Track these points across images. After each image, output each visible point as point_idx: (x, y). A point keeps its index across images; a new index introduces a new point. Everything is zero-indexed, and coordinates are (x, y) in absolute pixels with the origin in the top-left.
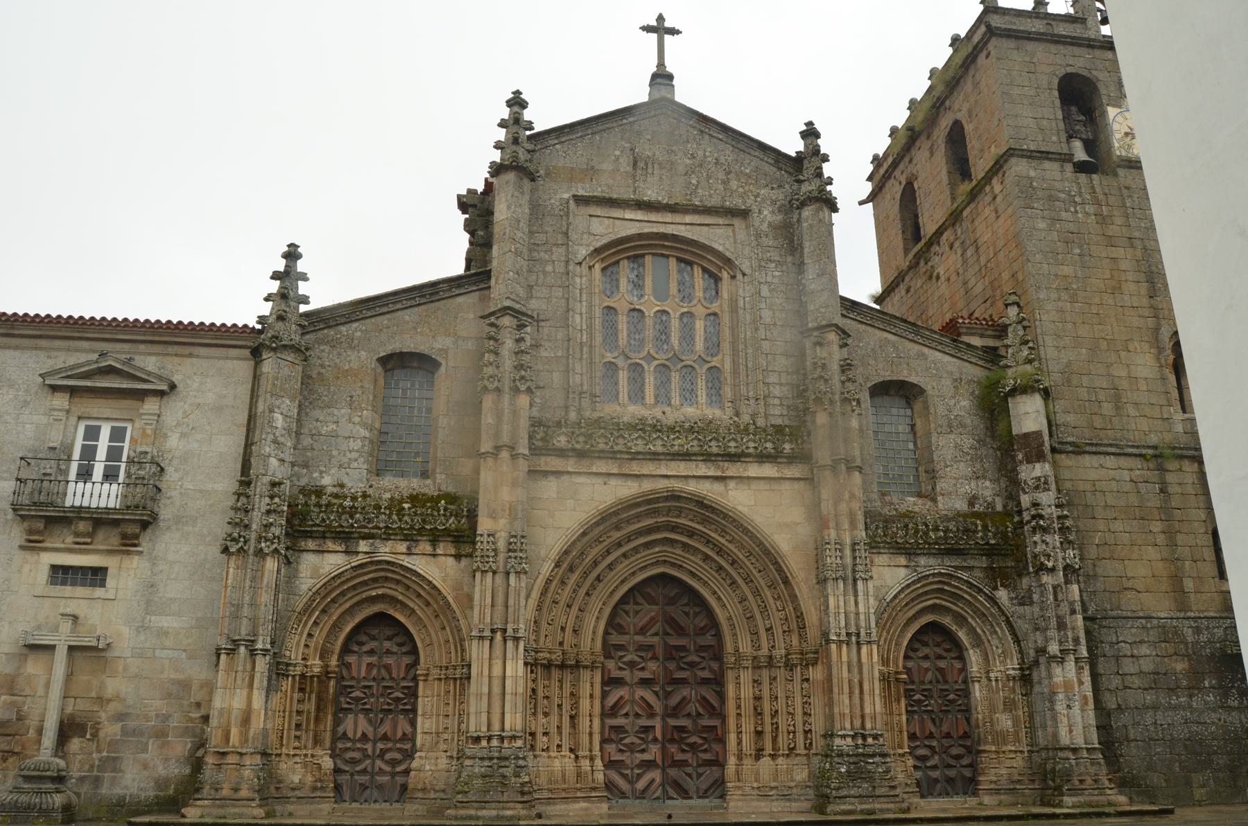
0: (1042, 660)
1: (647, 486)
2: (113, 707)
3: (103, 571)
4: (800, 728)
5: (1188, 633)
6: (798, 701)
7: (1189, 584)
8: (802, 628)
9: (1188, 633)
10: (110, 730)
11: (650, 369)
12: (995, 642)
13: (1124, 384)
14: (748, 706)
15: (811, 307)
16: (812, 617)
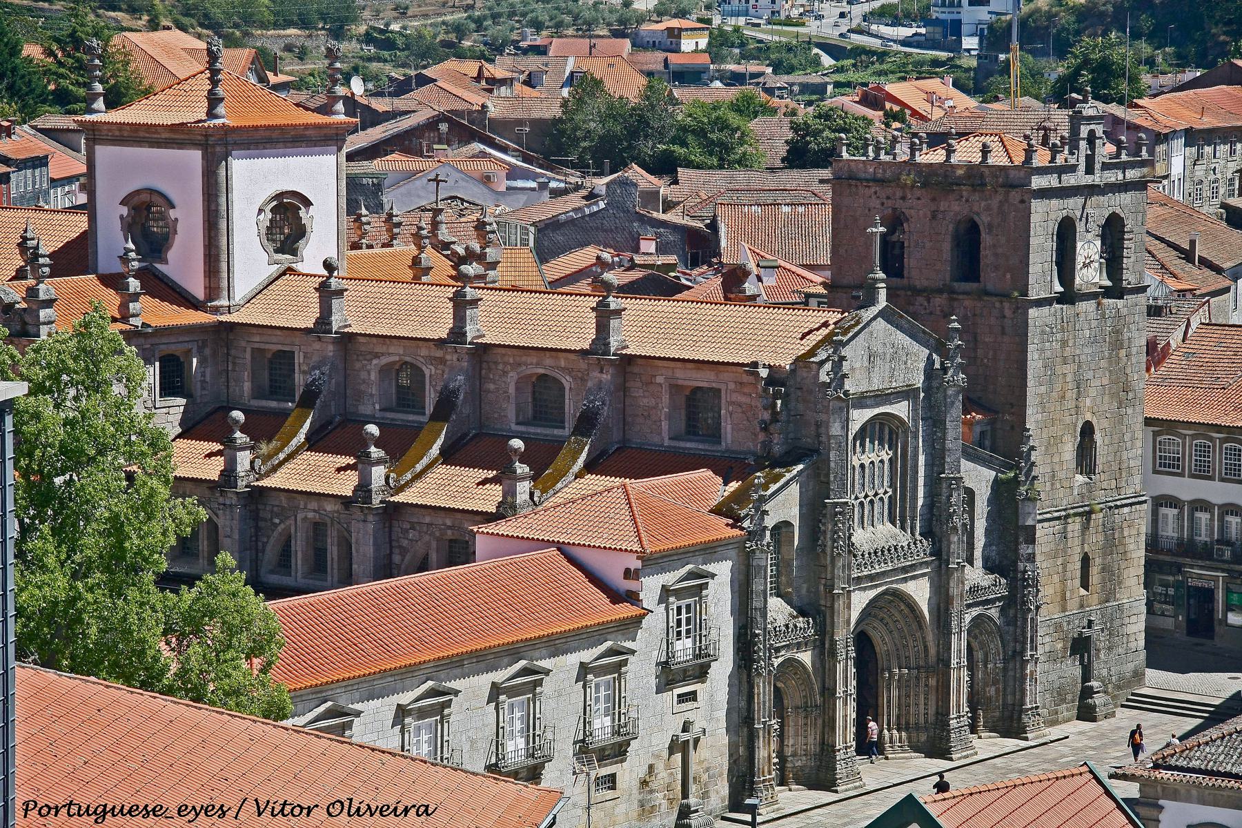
0: (1018, 658)
1: (880, 590)
2: (705, 765)
3: (694, 693)
4: (922, 711)
5: (1065, 624)
6: (922, 697)
7: (1068, 594)
8: (926, 656)
9: (1065, 624)
10: (705, 777)
11: (866, 502)
12: (992, 646)
13: (1057, 468)
14: (894, 701)
15: (948, 460)
16: (933, 651)
